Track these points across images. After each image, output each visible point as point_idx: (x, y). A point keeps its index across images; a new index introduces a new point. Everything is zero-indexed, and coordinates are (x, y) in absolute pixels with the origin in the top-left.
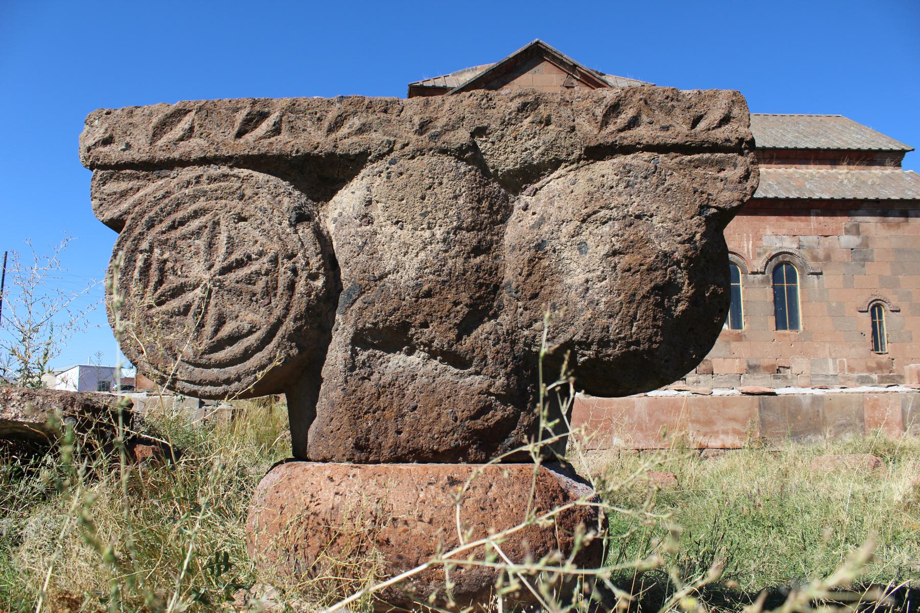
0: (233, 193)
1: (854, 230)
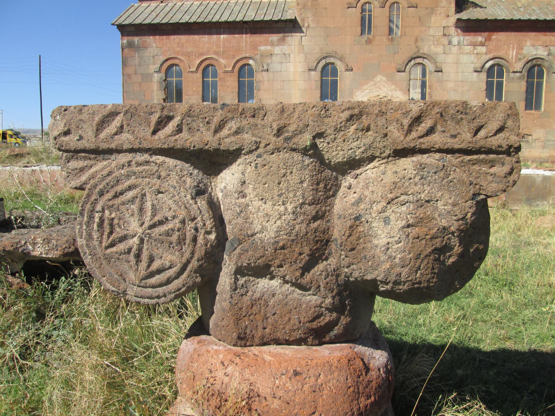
0: (153, 174)
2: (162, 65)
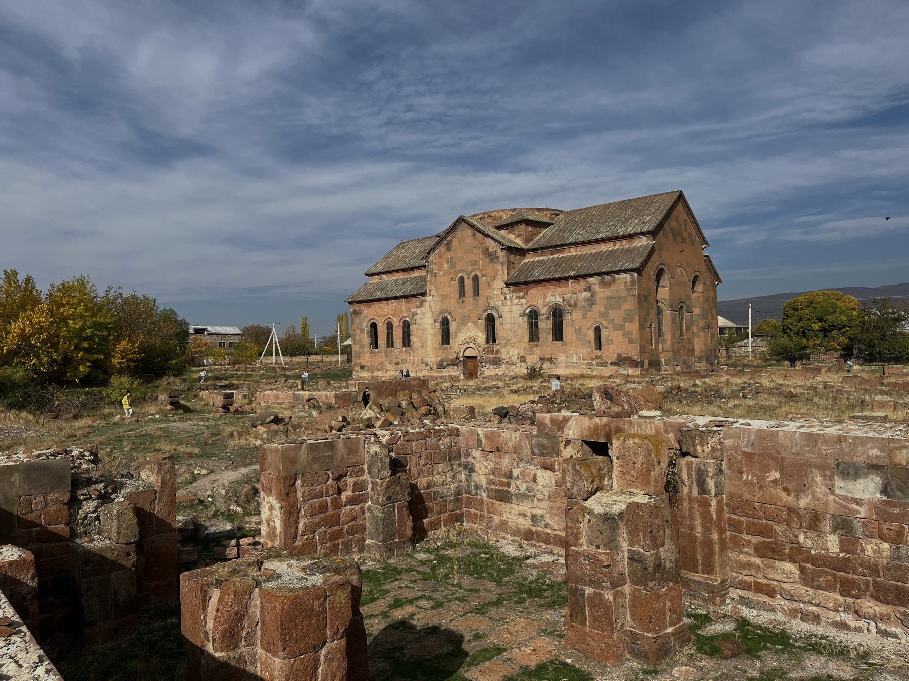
1: (588, 289)
2: (368, 323)
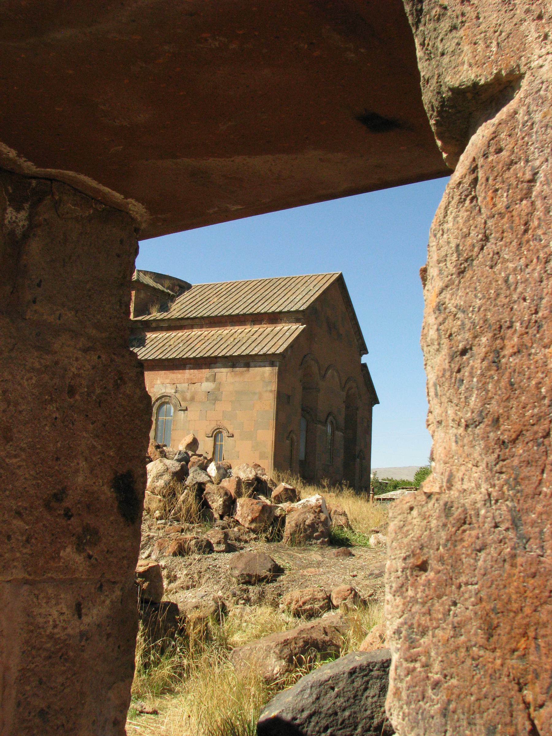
1: (212, 378)
